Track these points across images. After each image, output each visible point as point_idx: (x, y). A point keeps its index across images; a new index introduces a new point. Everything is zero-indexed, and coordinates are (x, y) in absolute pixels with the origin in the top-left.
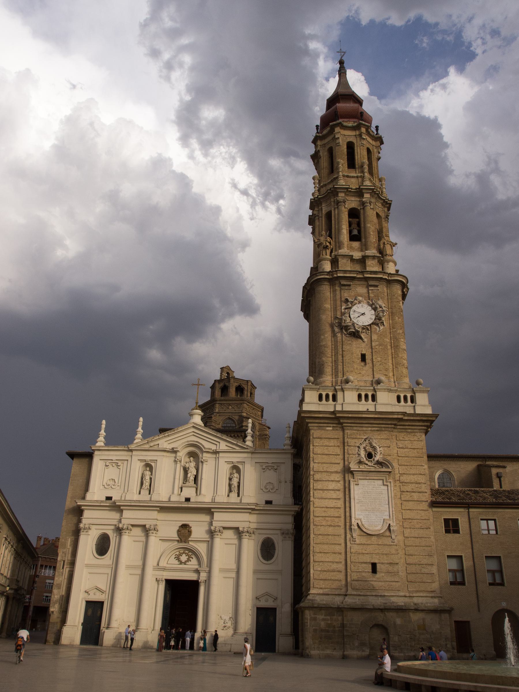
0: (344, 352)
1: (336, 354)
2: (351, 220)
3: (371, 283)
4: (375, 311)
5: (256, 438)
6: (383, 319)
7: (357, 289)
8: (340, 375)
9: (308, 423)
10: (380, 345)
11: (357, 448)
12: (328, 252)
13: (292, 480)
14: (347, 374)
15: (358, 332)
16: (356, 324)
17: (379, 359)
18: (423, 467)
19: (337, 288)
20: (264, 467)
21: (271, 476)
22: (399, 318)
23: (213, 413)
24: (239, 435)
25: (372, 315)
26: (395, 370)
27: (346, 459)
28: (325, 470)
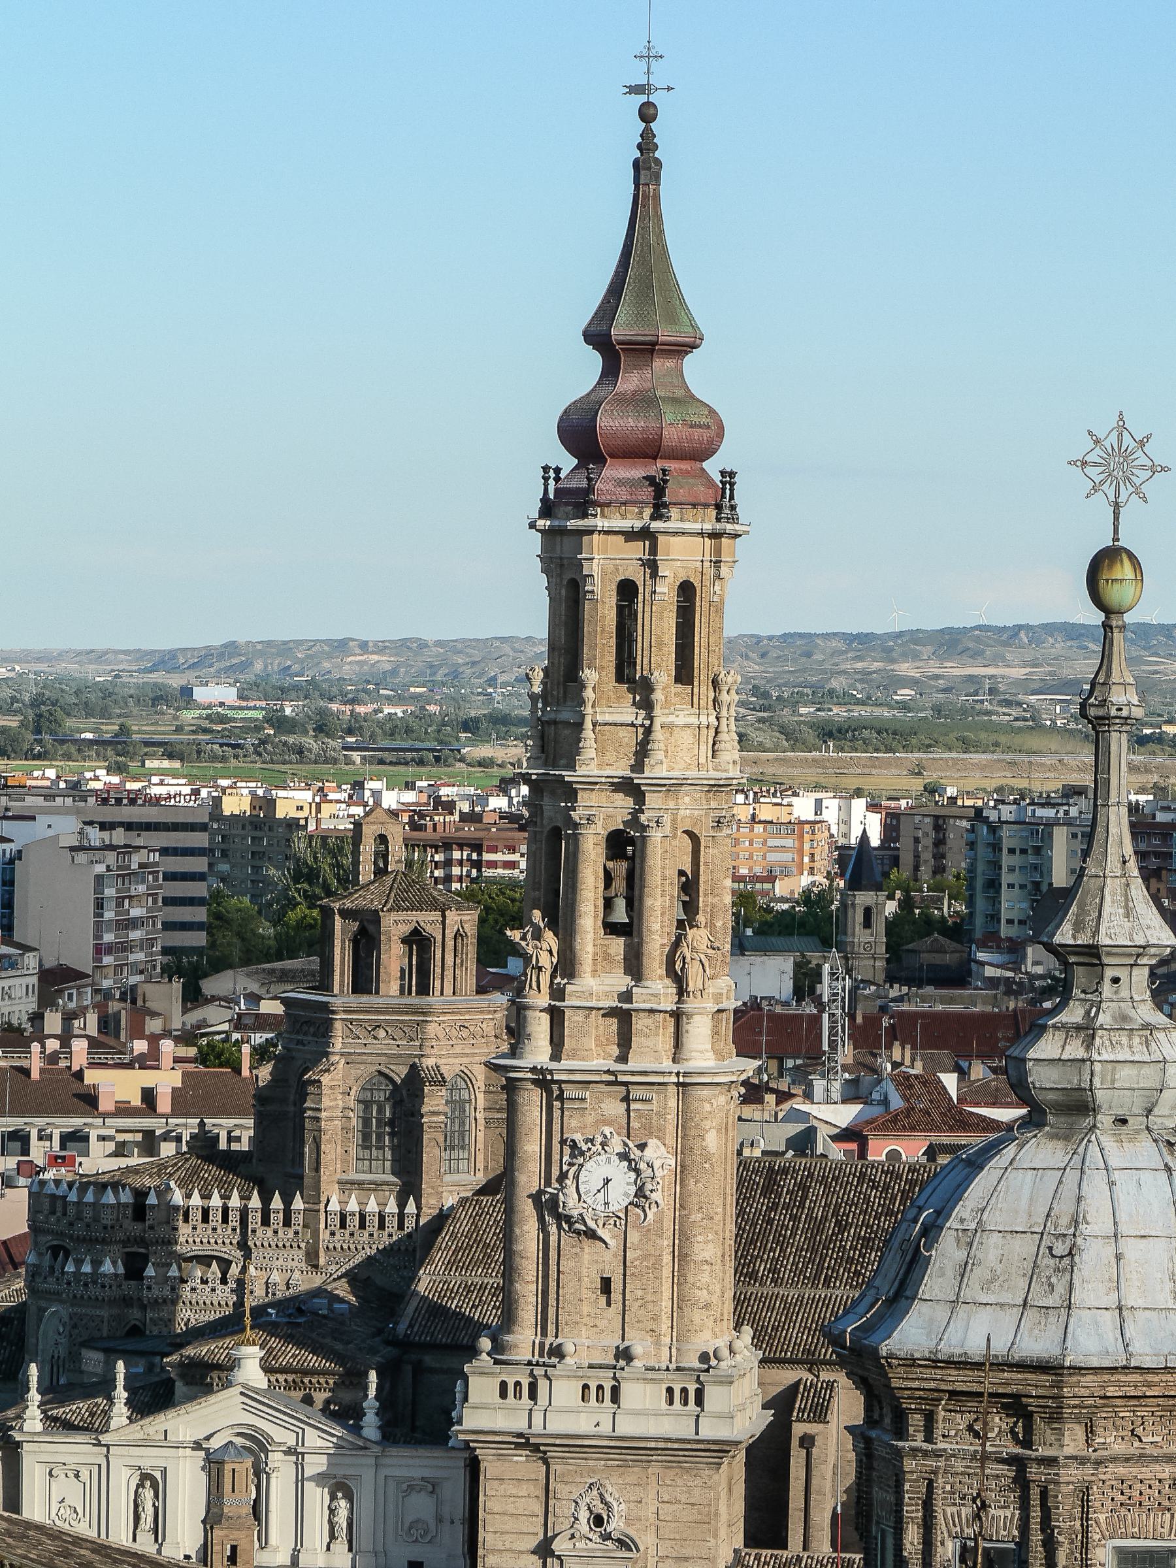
0: (561, 1276)
1: (546, 1276)
2: (610, 864)
3: (636, 1092)
4: (638, 1176)
5: (476, 1119)
6: (654, 1196)
7: (602, 1105)
8: (551, 1328)
9: (475, 1449)
10: (646, 1257)
11: (574, 1504)
12: (545, 978)
13: (467, 1515)
14: (567, 1329)
15: (594, 1231)
16: (590, 1209)
17: (639, 1293)
18: (708, 1544)
19: (557, 1104)
20: (404, 1486)
21: (421, 1506)
22: (697, 1181)
23: (327, 1055)
24: (355, 1382)
25: (628, 1184)
26: (675, 1314)
27: (550, 1525)
28: (508, 1546)
